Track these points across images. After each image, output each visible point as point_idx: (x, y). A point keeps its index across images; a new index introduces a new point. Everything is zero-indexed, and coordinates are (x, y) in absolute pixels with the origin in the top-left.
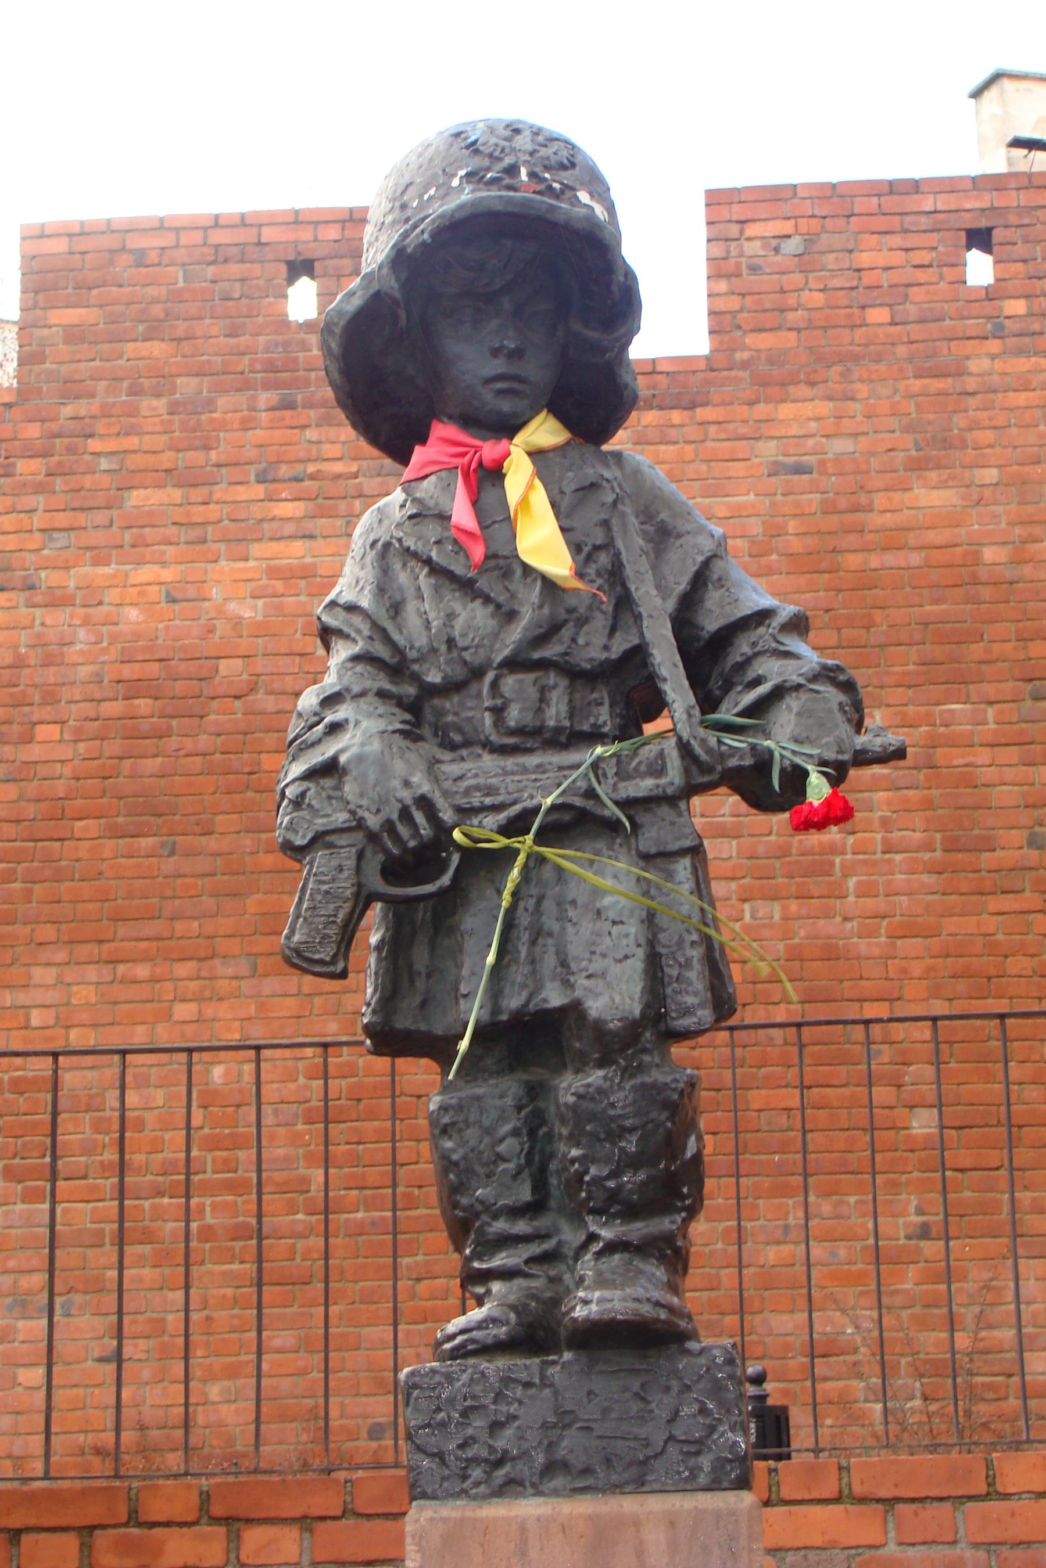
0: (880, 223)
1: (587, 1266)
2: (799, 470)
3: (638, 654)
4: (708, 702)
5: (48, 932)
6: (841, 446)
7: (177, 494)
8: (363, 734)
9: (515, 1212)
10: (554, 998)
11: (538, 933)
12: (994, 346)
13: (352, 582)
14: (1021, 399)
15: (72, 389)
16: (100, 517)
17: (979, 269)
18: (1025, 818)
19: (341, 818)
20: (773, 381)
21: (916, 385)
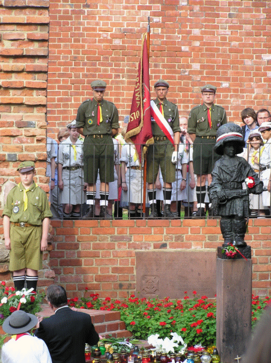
9: (229, 232)
10: (235, 213)
11: (233, 207)
19: (216, 196)
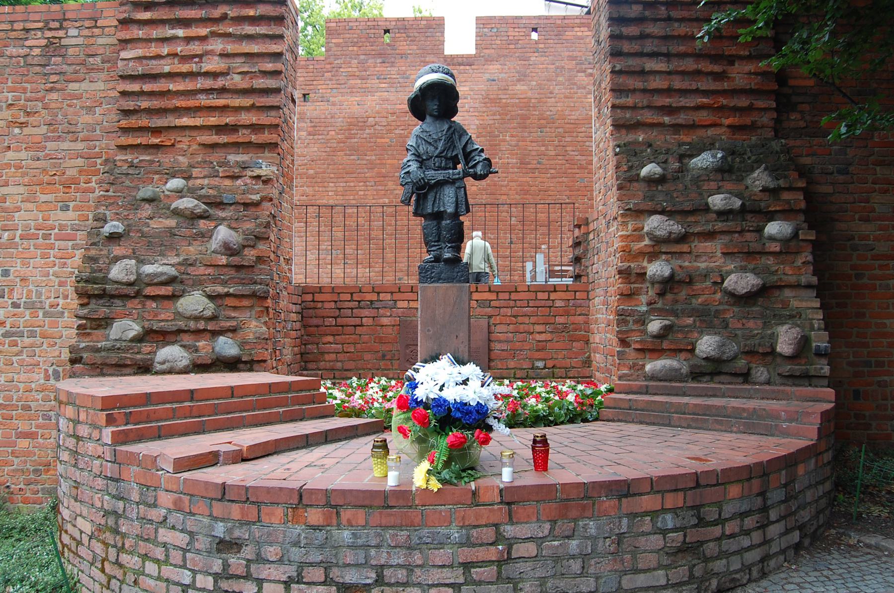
0: (514, 26)
1: (446, 250)
2: (494, 80)
3: (457, 155)
4: (467, 163)
5: (332, 175)
6: (503, 75)
7: (360, 81)
8: (414, 166)
10: (442, 209)
12: (536, 54)
13: (411, 142)
14: (541, 66)
15: (337, 57)
16: (343, 86)
17: (534, 36)
18: (537, 158)
20: (489, 60)
21: (520, 62)
